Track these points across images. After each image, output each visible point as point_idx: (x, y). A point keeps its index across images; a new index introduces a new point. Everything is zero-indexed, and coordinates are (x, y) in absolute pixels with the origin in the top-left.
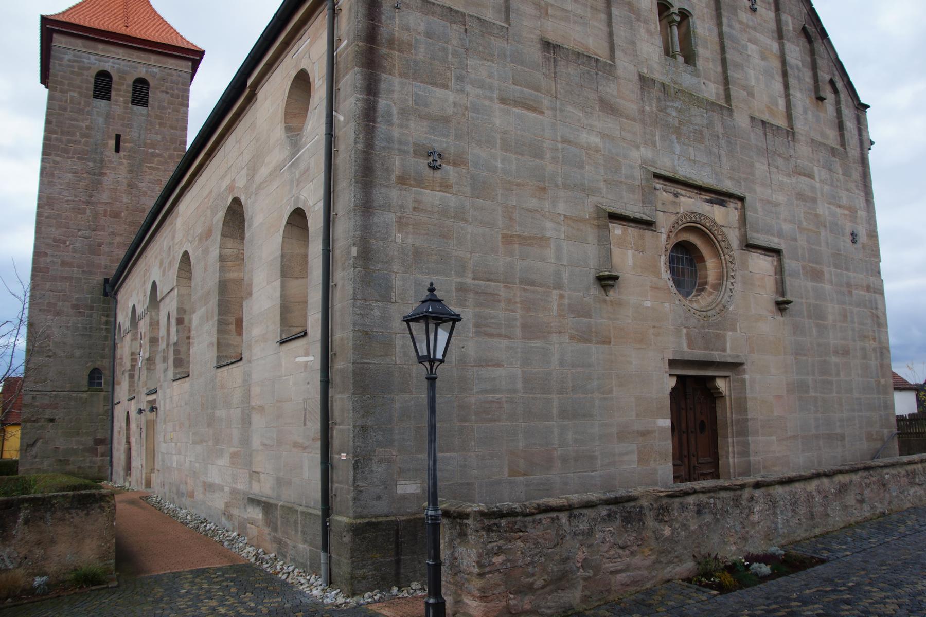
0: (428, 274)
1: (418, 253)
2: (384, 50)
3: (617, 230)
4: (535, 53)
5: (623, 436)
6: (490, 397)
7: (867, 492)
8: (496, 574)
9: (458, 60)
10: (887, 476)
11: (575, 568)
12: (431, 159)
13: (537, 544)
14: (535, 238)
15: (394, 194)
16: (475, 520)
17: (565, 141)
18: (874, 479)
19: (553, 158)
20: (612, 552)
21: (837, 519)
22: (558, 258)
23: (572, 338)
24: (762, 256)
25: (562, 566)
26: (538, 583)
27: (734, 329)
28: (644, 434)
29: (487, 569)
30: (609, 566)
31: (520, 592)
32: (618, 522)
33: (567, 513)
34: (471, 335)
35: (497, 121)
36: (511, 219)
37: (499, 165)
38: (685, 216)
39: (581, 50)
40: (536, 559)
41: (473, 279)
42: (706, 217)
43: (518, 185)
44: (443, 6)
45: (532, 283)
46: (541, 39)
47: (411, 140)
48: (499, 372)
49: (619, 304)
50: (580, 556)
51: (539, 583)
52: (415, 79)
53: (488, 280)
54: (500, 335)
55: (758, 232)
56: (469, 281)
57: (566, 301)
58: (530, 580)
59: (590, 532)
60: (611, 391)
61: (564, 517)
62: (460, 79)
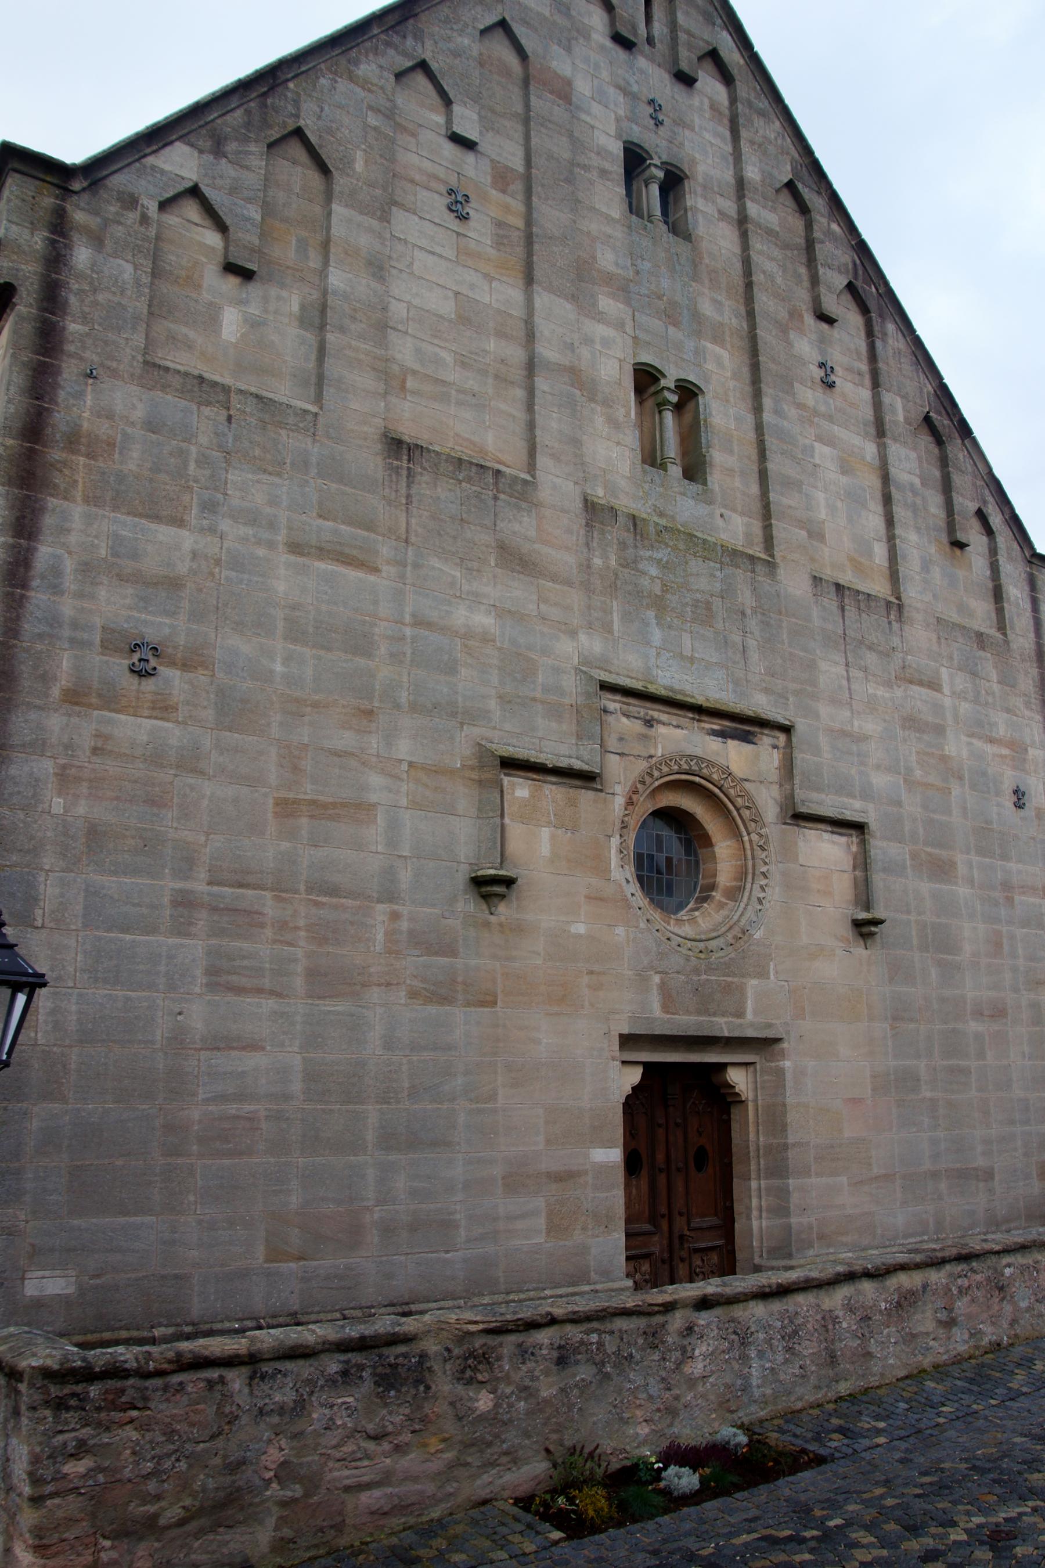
0: (115, 873)
1: (94, 833)
2: (56, 455)
3: (520, 789)
4: (370, 460)
5: (516, 1180)
6: (232, 1108)
7: (961, 1306)
8: (71, 1498)
9: (207, 472)
10: (1008, 1271)
11: (257, 1482)
12: (136, 657)
13: (170, 1433)
14: (344, 805)
15: (55, 722)
16: (31, 1385)
17: (419, 622)
18: (978, 1277)
19: (392, 655)
20: (349, 1448)
21: (890, 1359)
22: (392, 843)
23: (413, 994)
25: (229, 1479)
26: (168, 1514)
27: (763, 974)
29: (49, 1489)
30: (344, 1475)
31: (127, 1534)
32: (367, 1386)
33: (245, 1371)
34: (197, 990)
35: (281, 587)
36: (295, 768)
37: (279, 668)
38: (666, 761)
39: (466, 453)
40: (167, 1464)
41: (209, 884)
42: (711, 764)
43: (315, 705)
44: (186, 374)
45: (333, 891)
46: (385, 435)
47: (98, 621)
49: (519, 929)
50: (273, 1456)
51: (172, 1513)
52: (115, 508)
53: (241, 885)
54: (259, 991)
55: (819, 790)
56: (199, 886)
57: (404, 925)
58: (152, 1509)
59: (300, 1407)
60: (492, 1097)
61: (236, 1380)
62: (210, 507)
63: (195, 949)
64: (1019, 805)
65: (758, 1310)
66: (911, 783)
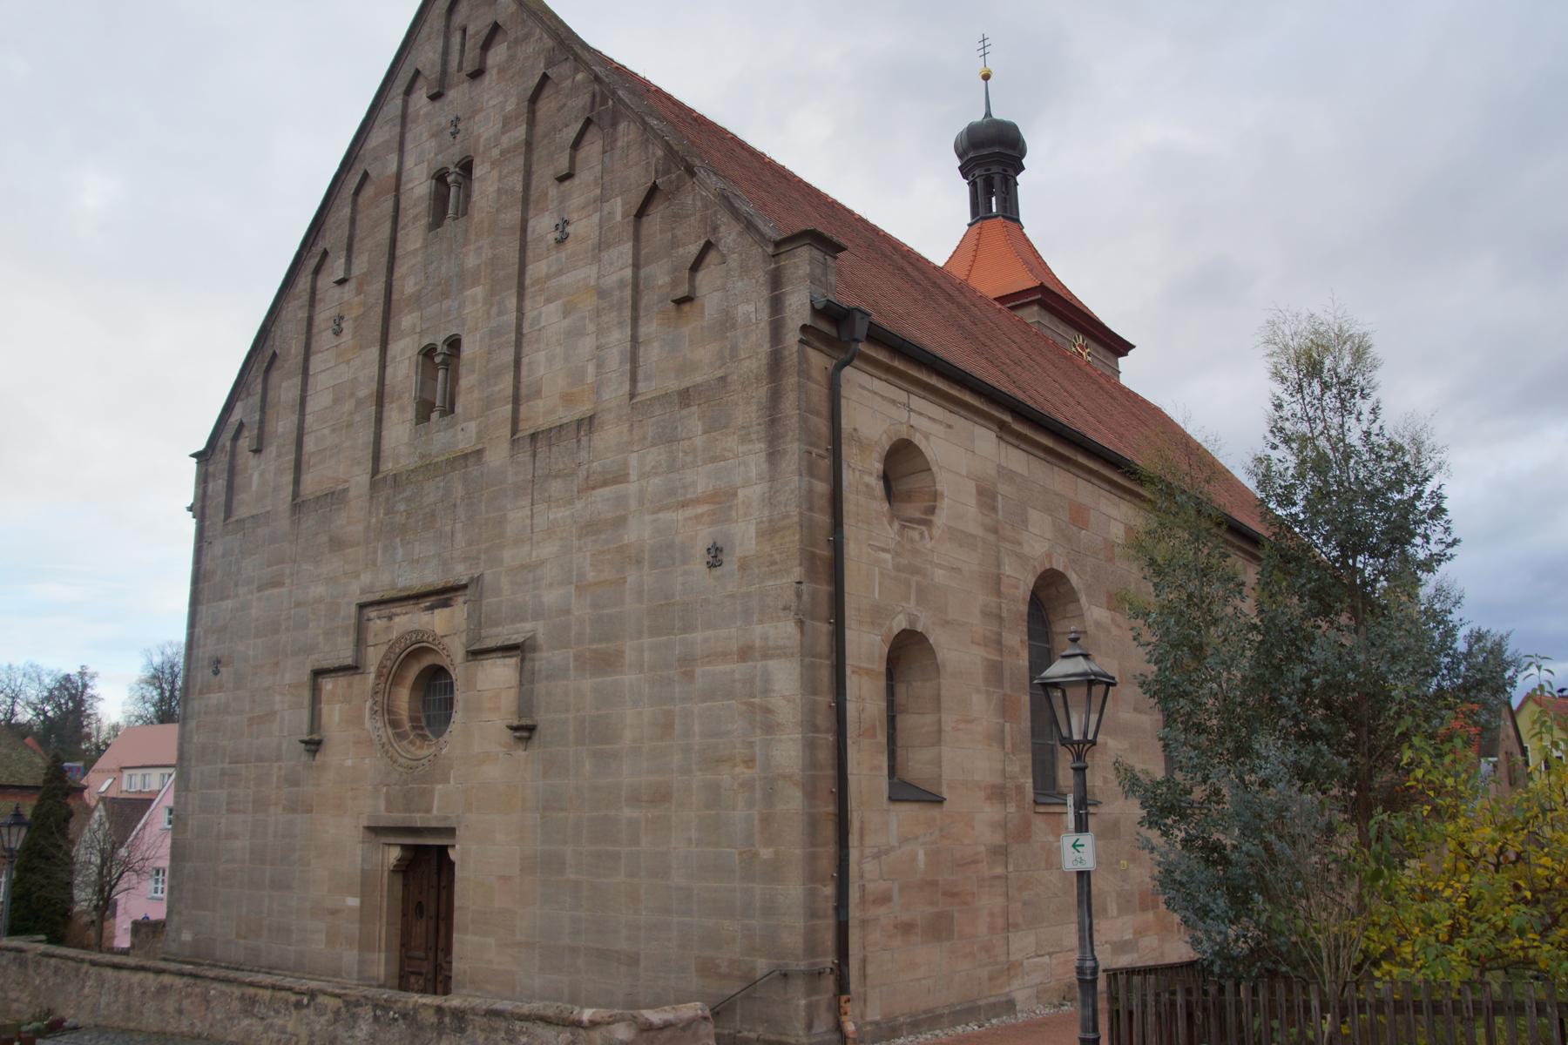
7: (186, 1004)
21: (151, 1021)
24: (499, 661)
27: (446, 780)
28: (334, 912)
38: (398, 640)
42: (424, 632)
55: (498, 624)
56: (226, 766)
65: (109, 973)
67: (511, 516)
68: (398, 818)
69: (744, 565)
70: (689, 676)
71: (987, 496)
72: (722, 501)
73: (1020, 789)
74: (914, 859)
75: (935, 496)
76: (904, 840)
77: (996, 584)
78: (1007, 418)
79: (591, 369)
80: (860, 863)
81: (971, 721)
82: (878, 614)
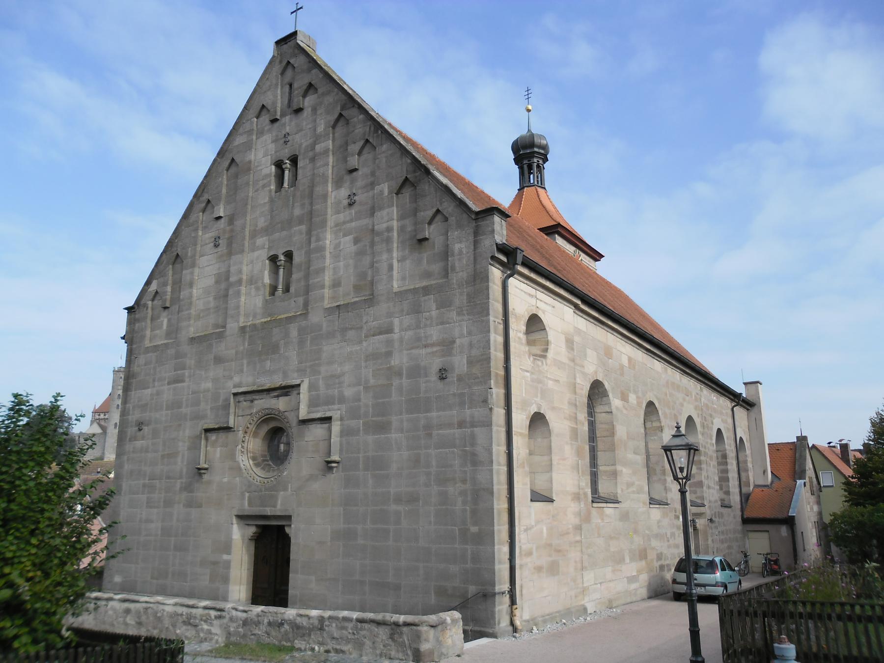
3: (213, 437)
23: (184, 506)
27: (285, 489)
28: (215, 563)
42: (273, 409)
48: (153, 526)
49: (209, 482)
63: (144, 497)
64: (442, 378)
66: (366, 388)
67: (325, 348)
68: (256, 510)
69: (460, 379)
70: (430, 435)
71: (570, 343)
72: (447, 345)
73: (585, 494)
74: (542, 532)
75: (547, 343)
76: (538, 522)
77: (573, 387)
78: (579, 302)
79: (370, 272)
80: (519, 534)
81: (564, 459)
82: (525, 404)
